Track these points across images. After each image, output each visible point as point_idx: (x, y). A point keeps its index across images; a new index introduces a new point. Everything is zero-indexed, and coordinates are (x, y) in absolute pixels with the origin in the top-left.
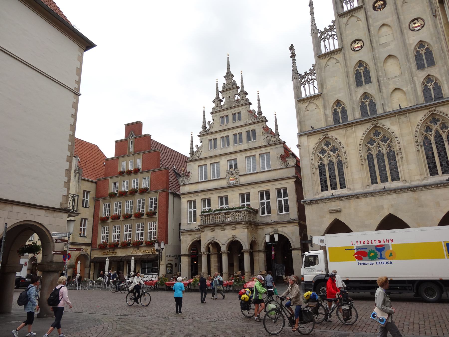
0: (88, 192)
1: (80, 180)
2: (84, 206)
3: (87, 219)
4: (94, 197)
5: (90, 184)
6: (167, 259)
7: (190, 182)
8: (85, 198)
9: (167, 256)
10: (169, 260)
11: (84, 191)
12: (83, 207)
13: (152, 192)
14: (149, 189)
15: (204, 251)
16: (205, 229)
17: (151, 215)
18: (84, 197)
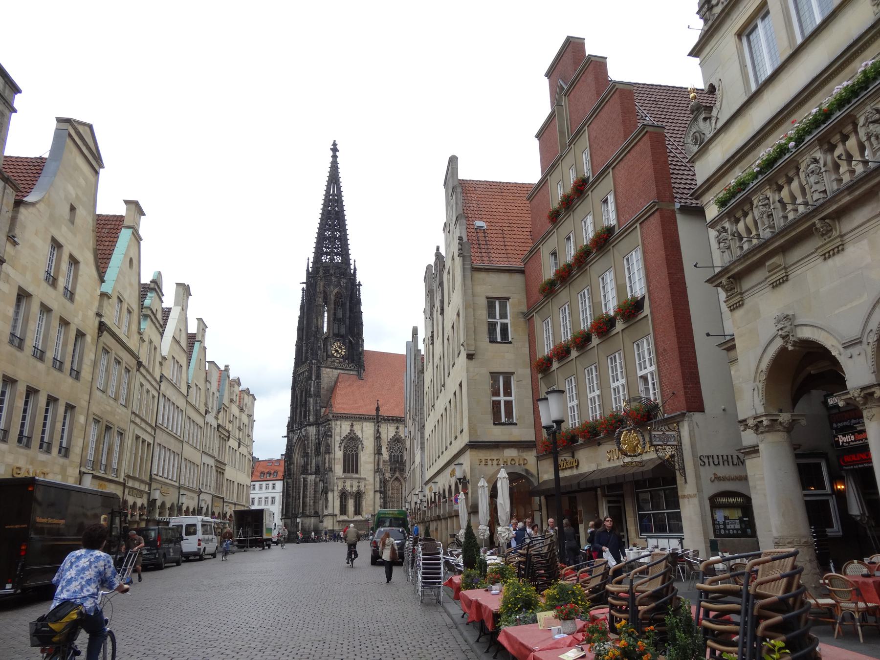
0: (504, 300)
1: (468, 273)
2: (499, 339)
3: (513, 374)
4: (524, 309)
5: (504, 278)
6: (708, 472)
7: (719, 125)
8: (498, 320)
9: (703, 460)
10: (718, 478)
11: (491, 301)
12: (493, 340)
13: (627, 231)
14: (617, 228)
15: (761, 410)
16: (747, 284)
17: (631, 310)
18: (491, 314)
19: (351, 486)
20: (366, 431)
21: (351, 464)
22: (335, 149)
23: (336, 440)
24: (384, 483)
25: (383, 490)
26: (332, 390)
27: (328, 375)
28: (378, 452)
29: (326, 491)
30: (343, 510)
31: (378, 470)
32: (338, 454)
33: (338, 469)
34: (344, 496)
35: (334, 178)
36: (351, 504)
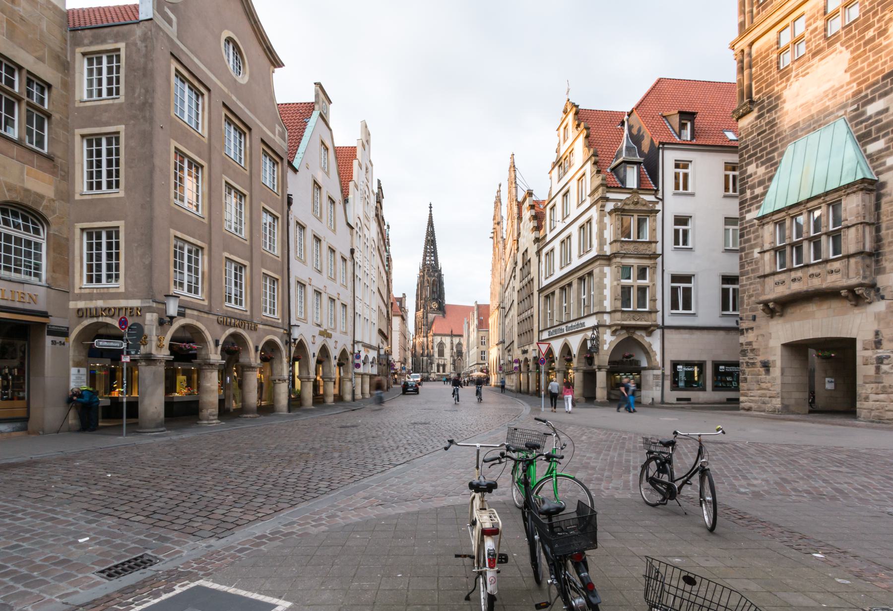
19: (441, 362)
20: (447, 340)
21: (441, 354)
22: (431, 207)
23: (436, 344)
24: (454, 361)
25: (454, 363)
26: (432, 323)
27: (431, 316)
28: (452, 349)
29: (431, 363)
30: (438, 371)
31: (452, 356)
32: (436, 349)
33: (436, 355)
34: (438, 366)
35: (431, 224)
36: (441, 368)
